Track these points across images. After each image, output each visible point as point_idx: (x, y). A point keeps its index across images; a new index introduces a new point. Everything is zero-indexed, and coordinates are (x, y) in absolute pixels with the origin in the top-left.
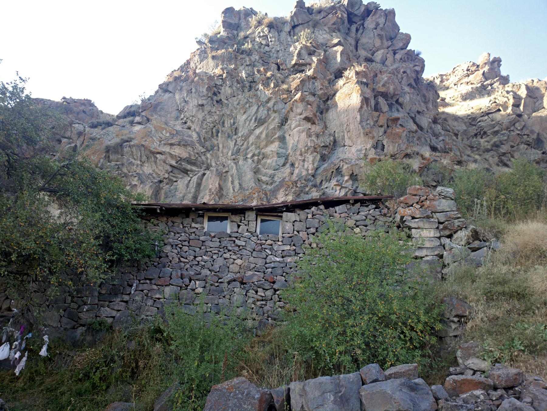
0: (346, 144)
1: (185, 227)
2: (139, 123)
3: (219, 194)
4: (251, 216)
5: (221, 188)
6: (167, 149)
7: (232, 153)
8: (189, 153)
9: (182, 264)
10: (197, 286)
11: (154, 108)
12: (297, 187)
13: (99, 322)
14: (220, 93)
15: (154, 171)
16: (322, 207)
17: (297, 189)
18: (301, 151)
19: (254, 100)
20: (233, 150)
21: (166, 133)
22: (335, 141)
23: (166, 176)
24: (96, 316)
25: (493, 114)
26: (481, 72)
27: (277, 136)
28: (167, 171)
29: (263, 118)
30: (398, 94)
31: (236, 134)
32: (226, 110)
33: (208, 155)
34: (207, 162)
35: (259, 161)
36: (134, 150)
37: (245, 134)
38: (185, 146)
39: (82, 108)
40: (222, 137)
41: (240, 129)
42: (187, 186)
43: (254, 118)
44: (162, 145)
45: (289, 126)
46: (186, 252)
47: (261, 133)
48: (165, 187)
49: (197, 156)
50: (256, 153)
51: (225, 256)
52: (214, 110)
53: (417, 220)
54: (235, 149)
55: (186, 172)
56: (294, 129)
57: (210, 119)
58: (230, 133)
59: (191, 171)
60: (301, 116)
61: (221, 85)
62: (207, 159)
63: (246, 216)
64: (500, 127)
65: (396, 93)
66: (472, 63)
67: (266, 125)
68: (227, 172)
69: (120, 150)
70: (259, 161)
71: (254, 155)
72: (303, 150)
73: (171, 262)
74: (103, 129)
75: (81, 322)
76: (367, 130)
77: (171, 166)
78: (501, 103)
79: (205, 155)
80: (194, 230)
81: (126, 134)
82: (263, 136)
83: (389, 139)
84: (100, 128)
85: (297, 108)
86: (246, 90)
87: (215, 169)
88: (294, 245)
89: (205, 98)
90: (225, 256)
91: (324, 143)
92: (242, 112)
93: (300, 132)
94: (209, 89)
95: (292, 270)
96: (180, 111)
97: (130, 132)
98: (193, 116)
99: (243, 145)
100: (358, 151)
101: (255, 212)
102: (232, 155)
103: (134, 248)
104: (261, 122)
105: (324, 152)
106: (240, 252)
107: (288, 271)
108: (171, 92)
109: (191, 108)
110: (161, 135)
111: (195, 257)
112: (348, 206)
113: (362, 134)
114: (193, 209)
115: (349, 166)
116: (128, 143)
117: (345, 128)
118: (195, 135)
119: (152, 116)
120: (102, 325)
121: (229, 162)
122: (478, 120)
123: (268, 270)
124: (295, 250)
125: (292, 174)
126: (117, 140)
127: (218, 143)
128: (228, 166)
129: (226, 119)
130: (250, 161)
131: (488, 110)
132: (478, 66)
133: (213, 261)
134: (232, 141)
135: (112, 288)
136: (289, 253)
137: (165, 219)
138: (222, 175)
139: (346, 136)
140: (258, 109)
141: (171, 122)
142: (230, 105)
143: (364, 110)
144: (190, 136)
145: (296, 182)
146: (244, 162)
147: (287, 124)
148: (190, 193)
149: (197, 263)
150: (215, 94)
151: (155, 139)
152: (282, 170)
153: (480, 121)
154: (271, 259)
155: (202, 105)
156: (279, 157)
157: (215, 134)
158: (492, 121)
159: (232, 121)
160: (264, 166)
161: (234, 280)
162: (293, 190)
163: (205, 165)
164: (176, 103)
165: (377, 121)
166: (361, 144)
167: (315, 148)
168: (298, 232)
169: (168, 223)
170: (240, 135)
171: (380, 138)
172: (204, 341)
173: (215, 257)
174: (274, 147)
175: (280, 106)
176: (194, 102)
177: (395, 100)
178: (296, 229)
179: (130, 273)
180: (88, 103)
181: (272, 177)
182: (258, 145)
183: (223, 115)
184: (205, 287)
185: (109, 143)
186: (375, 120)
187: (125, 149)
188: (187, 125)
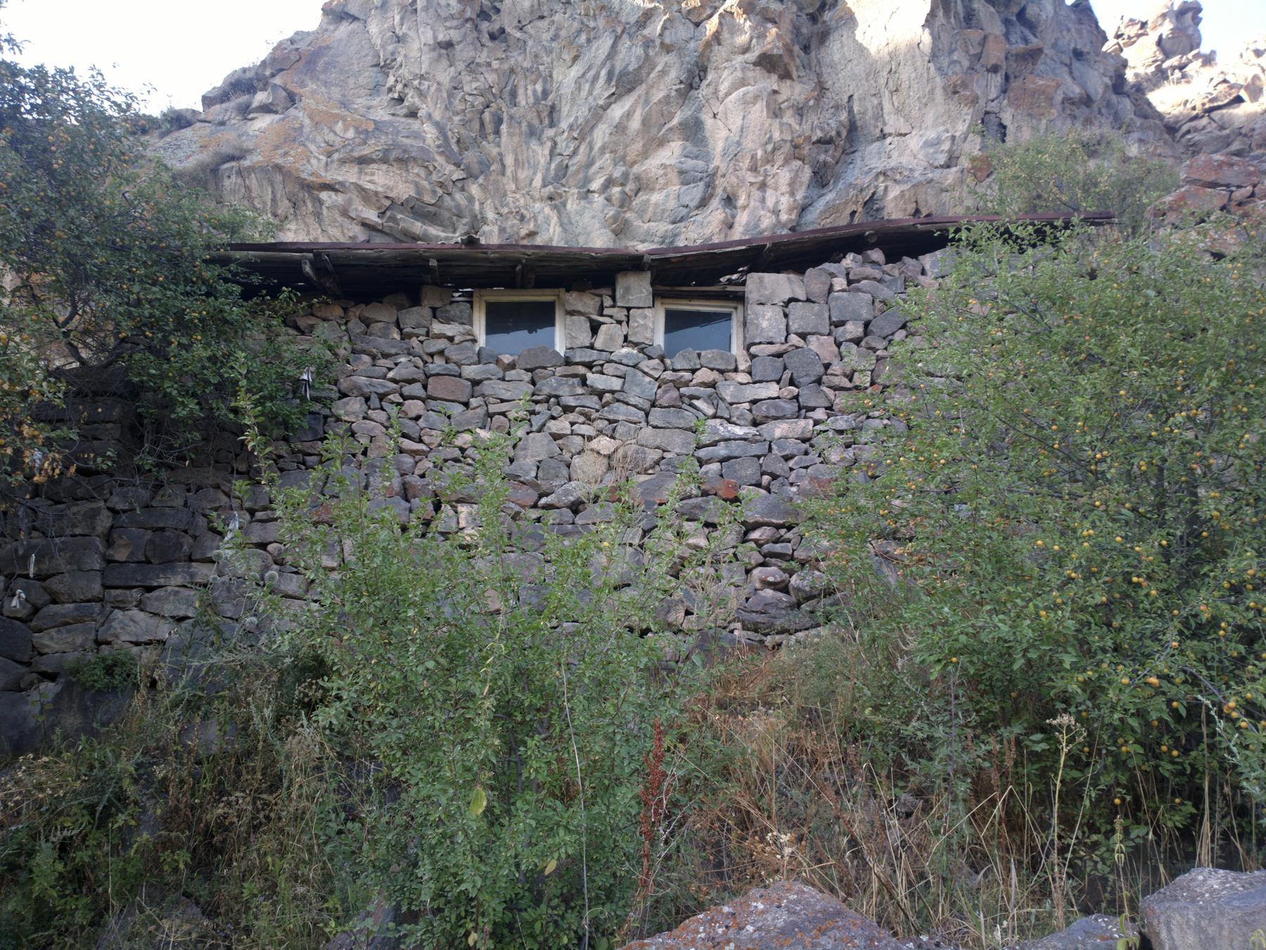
0: (887, 130)
1: (410, 336)
2: (266, 109)
4: (637, 289)
6: (349, 175)
7: (544, 180)
8: (416, 184)
9: (408, 460)
10: (463, 524)
11: (309, 62)
13: (104, 660)
14: (498, 11)
16: (877, 255)
18: (753, 157)
19: (601, 22)
20: (548, 169)
21: (346, 130)
22: (853, 127)
24: (98, 643)
25: (1224, 111)
26: (1153, 37)
27: (675, 122)
29: (631, 68)
31: (552, 125)
32: (520, 58)
33: (474, 189)
34: (471, 211)
35: (625, 201)
36: (253, 181)
37: (580, 121)
40: (511, 135)
41: (565, 110)
43: (603, 73)
44: (335, 165)
45: (711, 89)
46: (417, 418)
47: (629, 115)
49: (440, 191)
51: (554, 426)
52: (483, 57)
54: (553, 166)
56: (728, 94)
57: (474, 85)
58: (536, 122)
60: (747, 56)
62: (471, 199)
63: (619, 292)
64: (1244, 143)
66: (1126, 20)
67: (641, 90)
70: (625, 201)
71: (609, 183)
72: (760, 153)
73: (365, 453)
74: (162, 135)
75: (45, 665)
76: (954, 78)
78: (1241, 82)
79: (463, 189)
80: (441, 344)
82: (635, 124)
83: (1018, 107)
87: (496, 229)
88: (792, 382)
89: (455, 23)
90: (554, 426)
91: (822, 129)
92: (567, 57)
93: (746, 102)
95: (791, 463)
96: (384, 68)
97: (240, 136)
98: (422, 77)
99: (575, 153)
100: (928, 144)
101: (647, 276)
102: (544, 186)
103: (214, 380)
104: (625, 83)
105: (822, 157)
106: (606, 413)
107: (780, 468)
108: (355, 19)
109: (414, 53)
110: (331, 137)
113: (939, 93)
114: (433, 263)
115: (905, 187)
116: (234, 164)
117: (883, 81)
119: (303, 85)
120: (117, 670)
121: (538, 205)
122: (1185, 128)
123: (705, 468)
124: (796, 397)
125: (731, 226)
127: (500, 154)
128: (535, 218)
129: (522, 83)
130: (598, 199)
131: (1211, 101)
132: (1144, 25)
133: (514, 446)
134: (542, 144)
135: (151, 541)
136: (776, 407)
137: (338, 311)
140: (614, 46)
141: (360, 100)
142: (530, 43)
143: (937, 24)
144: (417, 135)
146: (583, 202)
147: (705, 83)
149: (457, 453)
150: (484, 15)
151: (312, 148)
152: (699, 218)
153: (1188, 132)
154: (716, 432)
155: (449, 45)
157: (489, 128)
158: (1222, 128)
159: (539, 87)
160: (641, 213)
163: (465, 221)
164: (373, 46)
165: (978, 57)
166: (935, 125)
167: (796, 147)
168: (803, 336)
169: (350, 325)
170: (564, 125)
171: (993, 107)
172: (521, 675)
174: (671, 153)
175: (682, 31)
176: (422, 37)
177: (1016, 10)
178: (794, 327)
179: (218, 487)
182: (620, 153)
183: (512, 71)
186: (972, 51)
187: (227, 182)
188: (406, 103)
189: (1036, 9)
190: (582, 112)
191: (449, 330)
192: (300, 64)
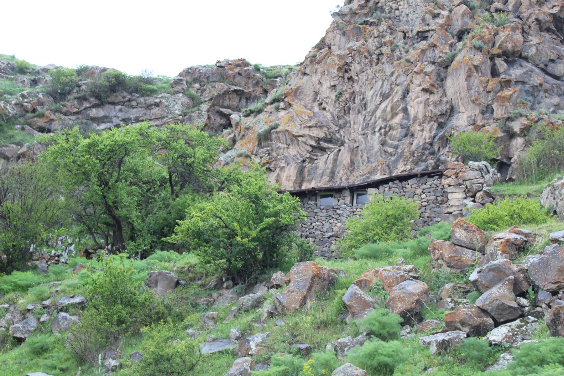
2: (284, 109)
3: (350, 168)
5: (352, 162)
6: (306, 132)
8: (325, 133)
11: (295, 93)
12: (414, 156)
15: (298, 152)
17: (415, 158)
23: (308, 155)
28: (308, 151)
30: (518, 51)
35: (386, 134)
36: (280, 135)
37: (372, 110)
38: (320, 127)
39: (237, 70)
41: (369, 104)
42: (326, 163)
43: (379, 93)
47: (387, 107)
48: (308, 165)
50: (383, 126)
51: (330, 221)
53: (451, 187)
55: (323, 150)
58: (361, 109)
59: (329, 148)
61: (351, 63)
62: (341, 136)
65: (516, 50)
67: (390, 98)
68: (357, 147)
69: (269, 137)
70: (386, 134)
71: (381, 129)
74: (255, 117)
77: (311, 146)
81: (273, 121)
82: (389, 109)
84: (252, 115)
85: (416, 79)
86: (374, 65)
90: (330, 221)
92: (369, 88)
94: (339, 69)
99: (371, 119)
104: (385, 97)
106: (340, 218)
108: (308, 74)
110: (301, 119)
111: (311, 223)
112: (418, 179)
118: (329, 116)
125: (412, 144)
126: (266, 127)
130: (378, 134)
138: (354, 151)
139: (460, 103)
140: (382, 84)
142: (360, 81)
144: (325, 117)
145: (413, 153)
148: (328, 169)
150: (346, 71)
155: (335, 86)
156: (402, 128)
157: (347, 112)
159: (361, 97)
161: (333, 236)
162: (411, 160)
163: (340, 142)
170: (368, 110)
173: (324, 222)
174: (398, 119)
175: (402, 78)
176: (326, 84)
180: (243, 63)
181: (396, 147)
183: (353, 92)
184: (315, 241)
185: (260, 131)
186: (484, 85)
189: (526, 54)
191: (312, 203)
192: (293, 94)
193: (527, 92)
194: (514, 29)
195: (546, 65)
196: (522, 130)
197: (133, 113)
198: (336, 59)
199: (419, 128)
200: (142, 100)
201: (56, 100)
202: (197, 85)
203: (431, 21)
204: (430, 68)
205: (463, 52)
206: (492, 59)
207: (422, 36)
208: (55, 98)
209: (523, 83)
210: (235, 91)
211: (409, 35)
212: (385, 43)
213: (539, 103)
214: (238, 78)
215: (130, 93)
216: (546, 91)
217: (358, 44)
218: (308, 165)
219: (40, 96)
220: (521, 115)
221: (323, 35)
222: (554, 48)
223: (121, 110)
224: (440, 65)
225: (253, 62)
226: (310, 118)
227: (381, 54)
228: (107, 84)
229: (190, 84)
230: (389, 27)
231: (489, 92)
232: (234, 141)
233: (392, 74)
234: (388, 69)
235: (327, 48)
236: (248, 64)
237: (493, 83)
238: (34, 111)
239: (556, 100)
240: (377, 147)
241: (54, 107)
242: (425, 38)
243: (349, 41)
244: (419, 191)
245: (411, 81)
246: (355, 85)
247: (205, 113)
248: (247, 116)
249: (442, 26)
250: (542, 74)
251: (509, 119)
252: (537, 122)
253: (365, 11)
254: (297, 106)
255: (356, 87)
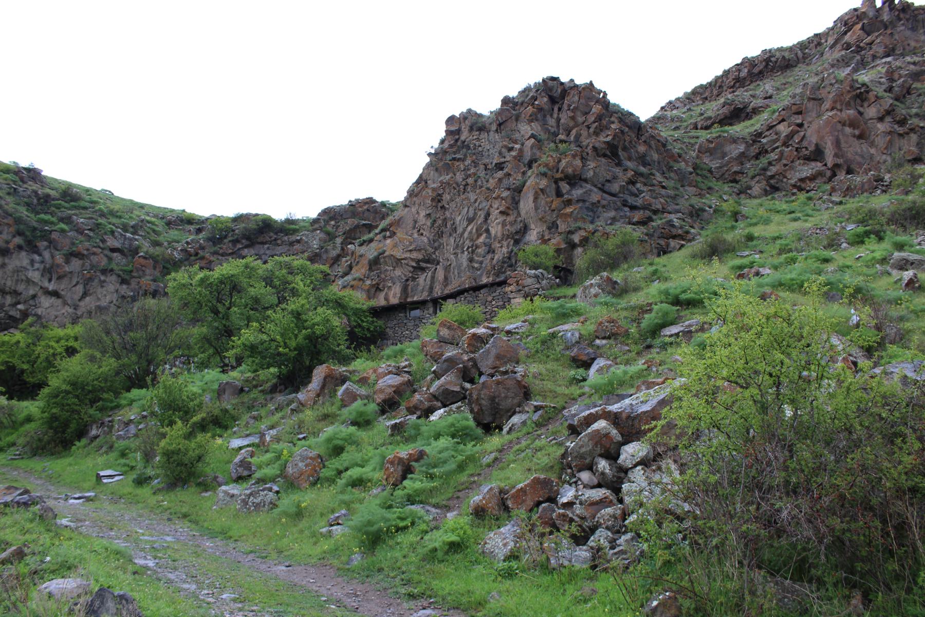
2: (390, 237)
4: (430, 305)
5: (446, 278)
6: (408, 255)
35: (473, 252)
38: (420, 250)
39: (365, 207)
48: (410, 283)
55: (423, 270)
59: (427, 268)
70: (473, 252)
71: (468, 248)
77: (413, 267)
82: (474, 231)
94: (433, 200)
104: (470, 221)
118: (425, 239)
126: (376, 254)
130: (466, 253)
138: (447, 269)
150: (439, 201)
174: (481, 239)
176: (423, 214)
180: (370, 201)
181: (481, 263)
190: (461, 230)
193: (587, 208)
194: (574, 156)
195: (603, 185)
196: (581, 241)
197: (279, 250)
198: (430, 191)
199: (498, 245)
200: (286, 238)
201: (215, 244)
202: (333, 223)
203: (507, 154)
204: (505, 194)
205: (532, 178)
206: (556, 182)
207: (500, 167)
208: (214, 243)
209: (584, 201)
210: (364, 225)
211: (490, 167)
212: (470, 176)
213: (598, 217)
214: (366, 214)
215: (276, 233)
216: (604, 207)
217: (448, 177)
218: (410, 283)
219: (202, 241)
220: (580, 229)
221: (421, 171)
222: (609, 171)
223: (268, 248)
224: (514, 190)
225: (379, 198)
226: (411, 243)
227: (467, 184)
228: (255, 227)
229: (327, 222)
230: (473, 161)
231: (553, 210)
232: (351, 267)
233: (476, 200)
234: (472, 197)
235: (423, 183)
236: (375, 202)
237: (557, 203)
238: (197, 254)
239: (612, 214)
240: (465, 263)
241: (213, 249)
242: (502, 169)
243: (441, 176)
244: (490, 299)
245: (491, 206)
246: (447, 213)
247: (339, 245)
248: (361, 245)
249: (515, 157)
250: (600, 193)
251: (571, 232)
252: (593, 233)
253: (454, 150)
254: (400, 234)
255: (448, 214)
